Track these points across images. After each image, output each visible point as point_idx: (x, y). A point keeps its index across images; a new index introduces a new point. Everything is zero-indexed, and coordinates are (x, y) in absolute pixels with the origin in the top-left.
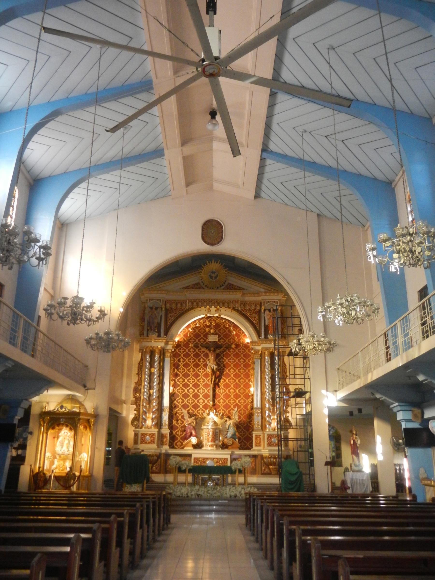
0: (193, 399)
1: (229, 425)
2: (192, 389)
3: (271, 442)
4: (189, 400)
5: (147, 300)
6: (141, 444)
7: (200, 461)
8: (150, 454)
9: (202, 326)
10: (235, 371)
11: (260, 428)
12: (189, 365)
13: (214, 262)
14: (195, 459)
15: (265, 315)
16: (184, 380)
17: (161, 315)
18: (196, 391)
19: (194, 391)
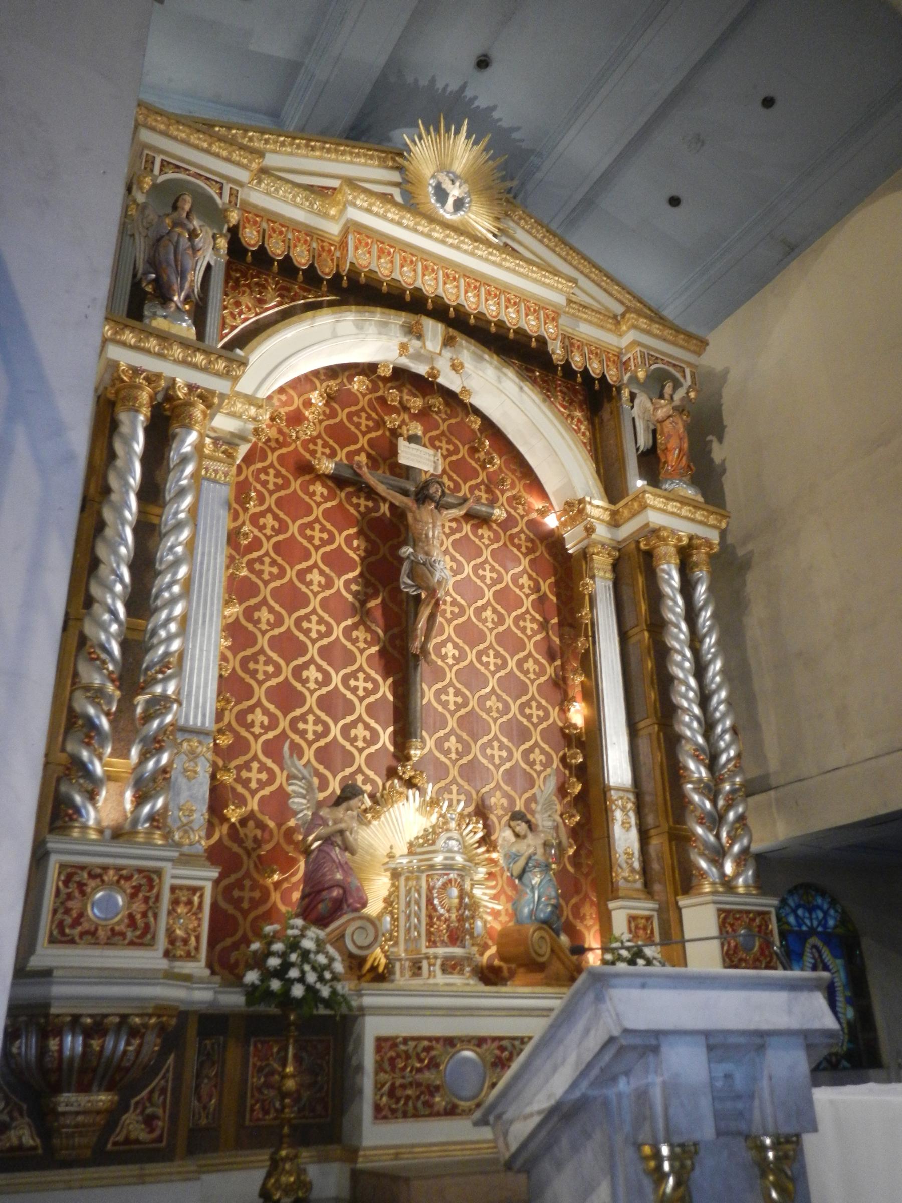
0: (323, 716)
1: (529, 858)
2: (319, 668)
3: (736, 947)
4: (303, 718)
5: (151, 162)
6: (52, 941)
7: (408, 1056)
8: (124, 1017)
9: (364, 402)
10: (501, 620)
11: (639, 885)
12: (307, 556)
13: (468, 137)
14: (381, 1042)
15: (636, 412)
16: (279, 621)
17: (209, 267)
18: (336, 679)
19: (327, 679)
